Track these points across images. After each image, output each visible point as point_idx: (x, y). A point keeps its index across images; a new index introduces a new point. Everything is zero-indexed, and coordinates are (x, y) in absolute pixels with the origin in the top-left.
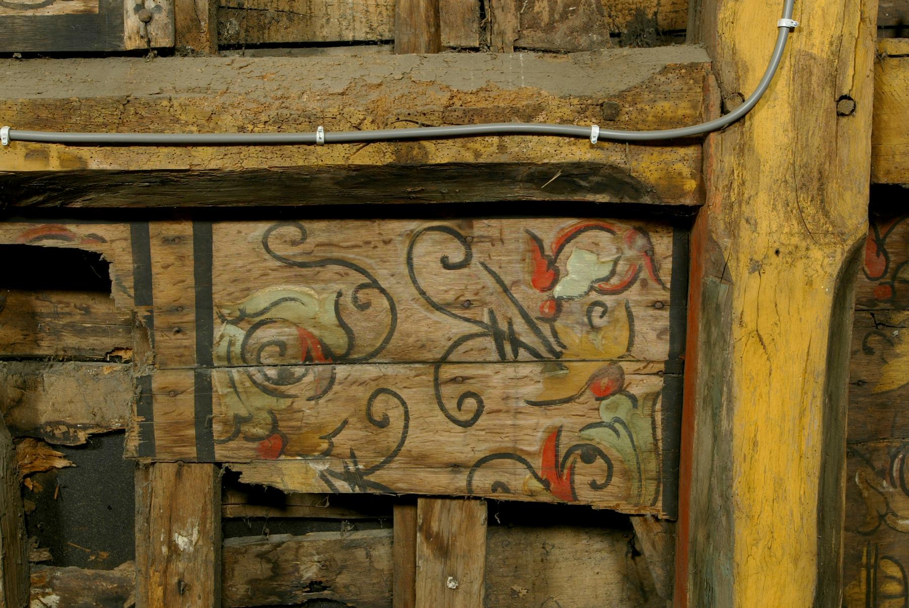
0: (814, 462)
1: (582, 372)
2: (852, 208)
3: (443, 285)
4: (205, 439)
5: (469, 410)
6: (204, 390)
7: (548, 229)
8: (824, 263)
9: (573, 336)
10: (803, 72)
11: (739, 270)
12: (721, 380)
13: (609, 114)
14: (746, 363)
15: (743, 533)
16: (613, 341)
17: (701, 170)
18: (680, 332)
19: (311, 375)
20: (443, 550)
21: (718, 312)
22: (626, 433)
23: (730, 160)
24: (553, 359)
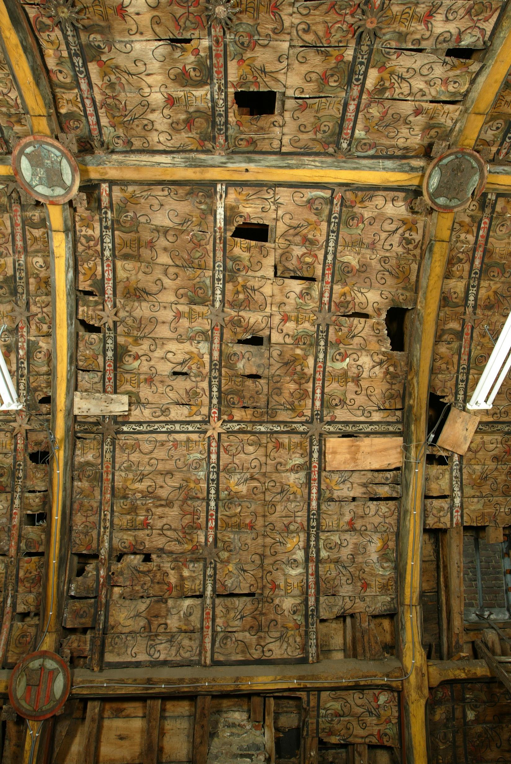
0: (425, 738)
1: (384, 718)
2: (426, 692)
3: (359, 702)
4: (318, 733)
5: (364, 726)
6: (318, 722)
7: (376, 692)
8: (423, 702)
9: (382, 712)
10: (416, 669)
11: (410, 704)
12: (409, 723)
13: (388, 676)
14: (413, 720)
15: (415, 752)
16: (388, 713)
17: (402, 684)
18: (400, 711)
19: (336, 720)
20: (360, 755)
21: (407, 711)
22: (392, 730)
24: (378, 716)
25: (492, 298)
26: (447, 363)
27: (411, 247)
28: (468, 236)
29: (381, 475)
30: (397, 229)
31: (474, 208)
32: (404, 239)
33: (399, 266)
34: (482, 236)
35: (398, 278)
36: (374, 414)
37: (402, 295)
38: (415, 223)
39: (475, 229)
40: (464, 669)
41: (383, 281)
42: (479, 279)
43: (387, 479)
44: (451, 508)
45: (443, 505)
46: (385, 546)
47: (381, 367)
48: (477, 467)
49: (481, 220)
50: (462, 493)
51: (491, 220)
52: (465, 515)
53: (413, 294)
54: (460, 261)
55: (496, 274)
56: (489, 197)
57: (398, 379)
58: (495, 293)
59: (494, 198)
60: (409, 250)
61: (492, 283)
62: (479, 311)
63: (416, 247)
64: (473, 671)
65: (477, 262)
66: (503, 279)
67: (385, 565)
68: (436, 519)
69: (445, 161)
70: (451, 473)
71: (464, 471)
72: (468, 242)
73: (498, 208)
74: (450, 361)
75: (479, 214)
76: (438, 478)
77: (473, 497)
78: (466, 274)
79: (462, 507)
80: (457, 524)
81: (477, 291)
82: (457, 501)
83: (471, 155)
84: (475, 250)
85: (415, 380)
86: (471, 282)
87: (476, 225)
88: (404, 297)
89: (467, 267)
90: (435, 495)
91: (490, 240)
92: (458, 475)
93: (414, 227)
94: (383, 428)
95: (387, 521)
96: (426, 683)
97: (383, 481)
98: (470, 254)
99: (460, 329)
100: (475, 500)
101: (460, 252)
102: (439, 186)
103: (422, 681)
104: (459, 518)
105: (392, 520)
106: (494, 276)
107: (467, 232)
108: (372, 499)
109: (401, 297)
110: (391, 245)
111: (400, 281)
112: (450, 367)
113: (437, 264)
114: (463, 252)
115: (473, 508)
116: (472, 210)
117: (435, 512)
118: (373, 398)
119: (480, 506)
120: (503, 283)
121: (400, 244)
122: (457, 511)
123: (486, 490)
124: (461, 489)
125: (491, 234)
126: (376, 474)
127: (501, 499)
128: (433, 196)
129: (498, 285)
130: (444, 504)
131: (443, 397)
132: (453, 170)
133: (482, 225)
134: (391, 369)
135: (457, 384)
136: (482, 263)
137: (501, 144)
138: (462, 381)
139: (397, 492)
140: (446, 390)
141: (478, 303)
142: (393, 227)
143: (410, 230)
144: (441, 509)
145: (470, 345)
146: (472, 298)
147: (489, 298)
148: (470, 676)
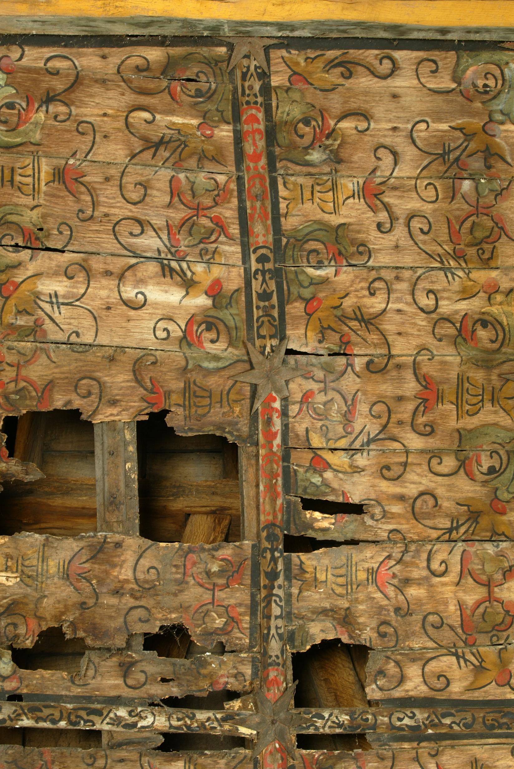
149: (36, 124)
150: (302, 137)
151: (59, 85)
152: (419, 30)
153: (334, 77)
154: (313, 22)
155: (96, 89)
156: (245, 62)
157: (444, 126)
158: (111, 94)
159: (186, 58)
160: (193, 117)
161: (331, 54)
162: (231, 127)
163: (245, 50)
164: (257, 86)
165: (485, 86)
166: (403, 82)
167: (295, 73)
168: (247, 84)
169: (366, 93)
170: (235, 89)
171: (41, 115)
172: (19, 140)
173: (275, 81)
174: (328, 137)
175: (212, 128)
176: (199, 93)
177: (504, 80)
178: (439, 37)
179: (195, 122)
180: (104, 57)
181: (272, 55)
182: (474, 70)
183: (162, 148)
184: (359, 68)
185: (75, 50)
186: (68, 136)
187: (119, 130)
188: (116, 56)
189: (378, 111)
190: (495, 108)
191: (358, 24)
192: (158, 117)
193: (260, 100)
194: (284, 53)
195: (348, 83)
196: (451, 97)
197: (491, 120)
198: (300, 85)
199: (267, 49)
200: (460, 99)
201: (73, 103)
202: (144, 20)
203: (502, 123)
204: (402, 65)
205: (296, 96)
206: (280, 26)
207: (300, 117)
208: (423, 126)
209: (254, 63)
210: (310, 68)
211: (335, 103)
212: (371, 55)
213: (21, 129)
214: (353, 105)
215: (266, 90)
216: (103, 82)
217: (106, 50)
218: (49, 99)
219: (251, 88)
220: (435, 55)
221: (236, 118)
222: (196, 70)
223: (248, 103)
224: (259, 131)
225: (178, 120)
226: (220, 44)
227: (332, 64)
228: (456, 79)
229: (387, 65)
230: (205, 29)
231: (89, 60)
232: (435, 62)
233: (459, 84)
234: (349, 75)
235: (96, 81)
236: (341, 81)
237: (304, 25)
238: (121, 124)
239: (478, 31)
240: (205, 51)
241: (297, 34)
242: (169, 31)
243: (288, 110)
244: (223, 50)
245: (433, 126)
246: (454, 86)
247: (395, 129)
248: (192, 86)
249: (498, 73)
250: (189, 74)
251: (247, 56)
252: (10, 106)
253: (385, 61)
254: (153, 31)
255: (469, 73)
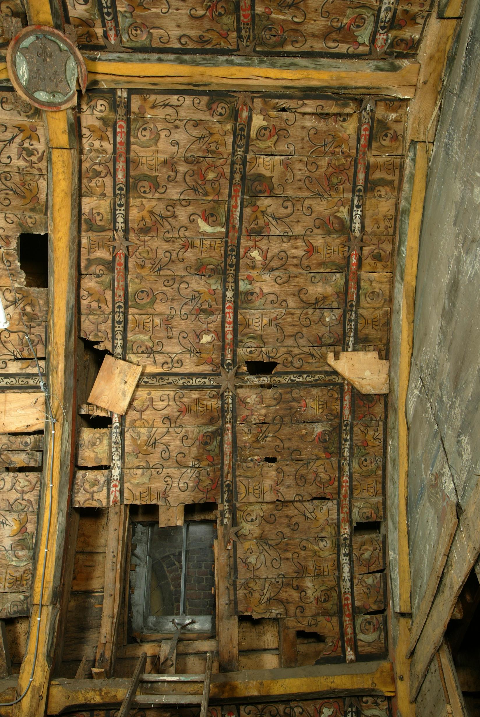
10: (33, 690)
23: (17, 711)
25: (147, 220)
26: (99, 301)
27: (34, 159)
28: (103, 143)
29: (19, 439)
30: (13, 138)
31: (103, 108)
32: (24, 149)
33: (24, 184)
34: (121, 143)
35: (24, 197)
36: (10, 364)
37: (30, 217)
38: (34, 129)
39: (110, 134)
40: (100, 690)
41: (8, 202)
42: (127, 196)
43: (26, 444)
44: (108, 482)
45: (99, 477)
46: (22, 529)
47: (16, 307)
48: (142, 430)
49: (115, 123)
50: (123, 463)
51: (128, 122)
52: (126, 491)
53: (42, 216)
54: (98, 174)
55: (147, 190)
56: (119, 93)
57: (38, 321)
58: (151, 213)
59: (125, 95)
60: (32, 163)
61: (145, 201)
62: (132, 236)
63: (40, 159)
64: (113, 693)
65: (120, 175)
66: (157, 195)
67: (20, 553)
68: (88, 496)
69: (26, 43)
70: (111, 438)
71: (127, 435)
72: (105, 151)
73: (134, 108)
74: (102, 298)
75: (112, 116)
76: (94, 444)
77: (138, 468)
78: (109, 191)
79: (121, 480)
80: (115, 502)
81: (127, 210)
82: (116, 473)
83: (53, 34)
84: (115, 161)
85: (51, 321)
86: (117, 200)
87: (110, 129)
88: (33, 220)
89: (108, 181)
90: (90, 465)
91: (133, 147)
92: (119, 440)
93: (33, 134)
94: (20, 382)
95: (26, 497)
96: (42, 708)
97: (22, 447)
98: (110, 165)
99: (111, 258)
100: (140, 471)
101: (96, 164)
102: (30, 78)
103: (38, 705)
104: (118, 494)
105: (31, 496)
106: (145, 192)
107: (101, 139)
108: (8, 470)
109: (29, 221)
110: (9, 157)
111: (27, 201)
112: (102, 305)
113: (61, 177)
114: (100, 164)
115: (136, 481)
116: (101, 111)
117: (87, 486)
118: (9, 346)
119: (145, 480)
120: (159, 199)
121: (20, 156)
122: (115, 486)
123: (155, 458)
124: (122, 458)
125: (132, 140)
126: (13, 438)
127: (173, 470)
128: (29, 90)
129: (154, 203)
130: (100, 476)
131: (97, 343)
132: (39, 55)
133: (118, 130)
134: (28, 309)
135: (113, 327)
136: (127, 175)
137: (104, 25)
138: (119, 323)
139: (36, 461)
140: (100, 334)
141: (131, 225)
142: (8, 135)
143: (30, 138)
144: (95, 483)
145: (126, 278)
146: (120, 220)
147: (143, 219)
148: (107, 700)
149: (348, 18)
150: (222, 7)
151: (334, 35)
152: (171, 61)
153: (208, 36)
154: (218, 66)
155: (317, 33)
156: (248, 44)
157: (153, 10)
158: (311, 30)
159: (275, 46)
160: (274, 18)
161: (209, 47)
162: (256, 12)
163: (248, 50)
164: (243, 32)
165: (136, 30)
166: (175, 33)
167: (225, 38)
168: (248, 33)
169: (192, 28)
170: (253, 31)
171: (345, 21)
172: (358, 10)
173: (235, 35)
174: (210, 6)
175: (265, 12)
176: (270, 29)
177: (128, 33)
178: (161, 55)
179: (273, 16)
180: (312, 47)
181: (236, 46)
182: (143, 38)
183: (290, 3)
184: (196, 40)
185: (324, 51)
186: (334, 11)
187: (309, 13)
188: (306, 48)
189: (186, 19)
190: (130, 19)
191: (198, 64)
192: (290, 19)
193: (242, 26)
194: (230, 47)
195: (201, 33)
196: (152, 25)
197: (131, 13)
198: (223, 32)
199: (238, 49)
200: (147, 24)
201: (329, 27)
202: (291, 68)
203: (125, 12)
204: (176, 41)
205: (225, 27)
206: (231, 63)
207: (223, 17)
208: (164, 11)
209: (244, 43)
210: (219, 40)
211: (207, 24)
212: (191, 46)
213: (355, 15)
214: (198, 22)
215: (239, 30)
216: (314, 36)
217: (310, 50)
218: (340, 29)
219: (246, 32)
220: (161, 46)
221: (253, 16)
222: (271, 41)
223: (248, 25)
224: (243, 10)
225: (281, 17)
226: (259, 52)
227: (209, 42)
228: (150, 34)
229: (183, 41)
230: (265, 62)
231: (319, 46)
232: (161, 42)
233: (149, 32)
234: (201, 37)
235: (317, 36)
236: (204, 34)
237: (222, 64)
238: (308, 16)
239: (145, 60)
240: (266, 49)
241: (224, 58)
242: (281, 61)
243: (228, 20)
244: (258, 49)
245: (158, 11)
246: (151, 31)
247: (177, 9)
248: (274, 33)
249: (131, 37)
250: (274, 39)
251: (247, 46)
252: (358, 27)
253: (184, 43)
254: (288, 60)
255: (144, 37)
